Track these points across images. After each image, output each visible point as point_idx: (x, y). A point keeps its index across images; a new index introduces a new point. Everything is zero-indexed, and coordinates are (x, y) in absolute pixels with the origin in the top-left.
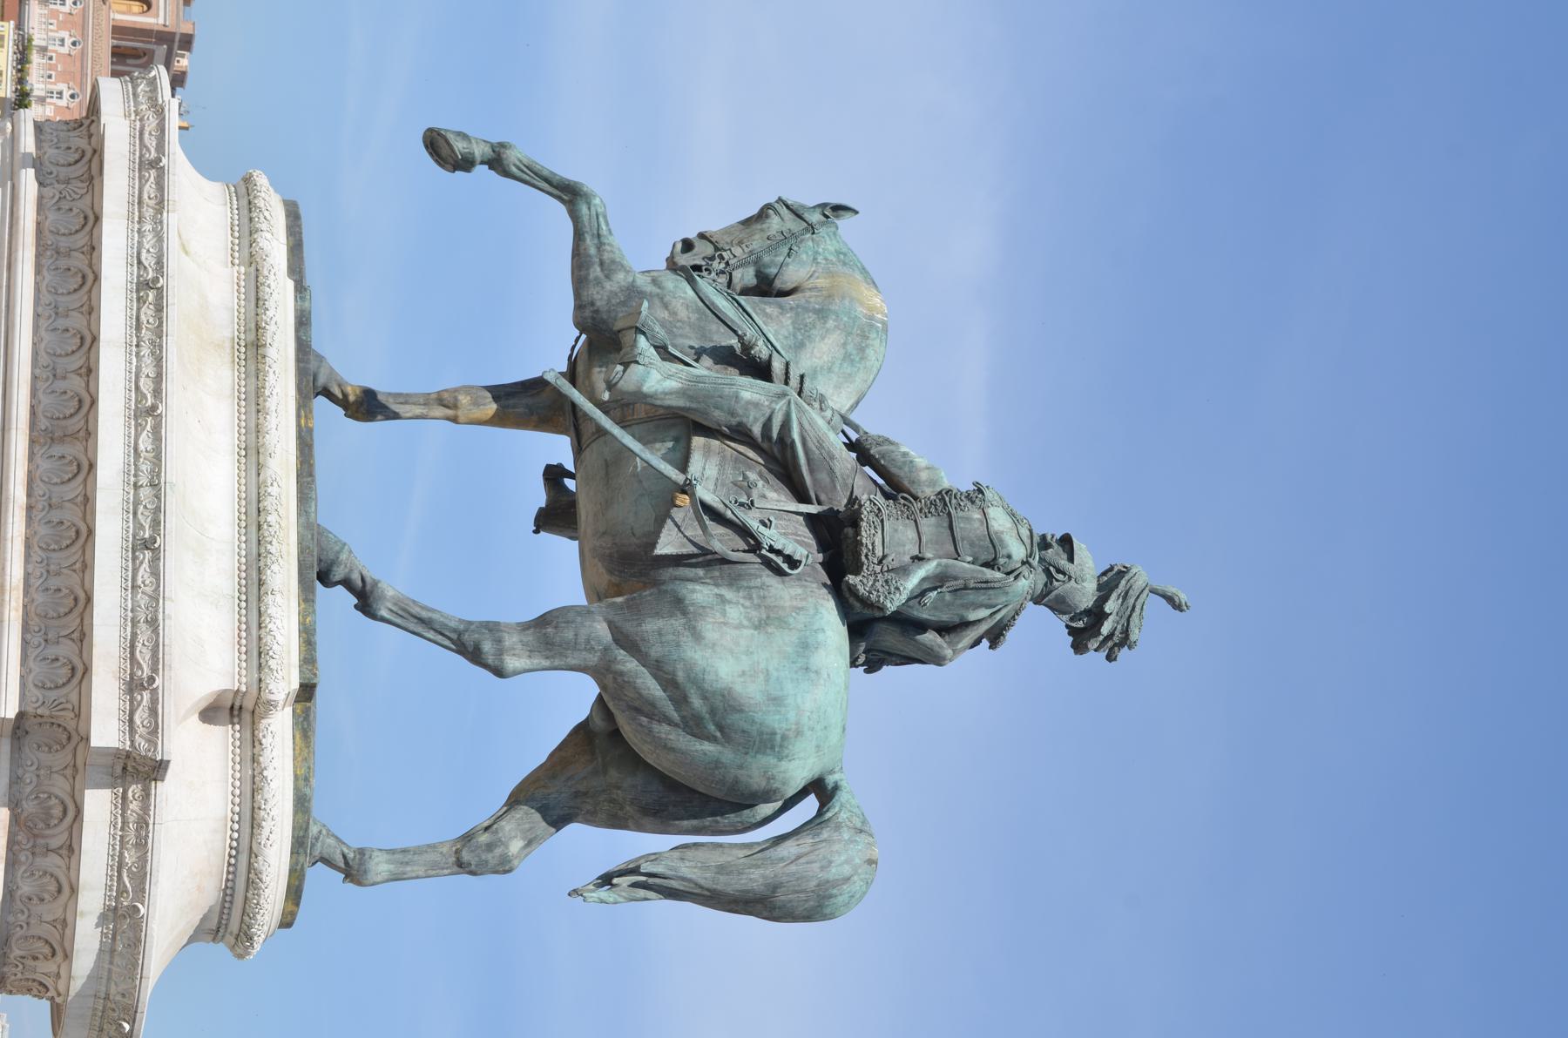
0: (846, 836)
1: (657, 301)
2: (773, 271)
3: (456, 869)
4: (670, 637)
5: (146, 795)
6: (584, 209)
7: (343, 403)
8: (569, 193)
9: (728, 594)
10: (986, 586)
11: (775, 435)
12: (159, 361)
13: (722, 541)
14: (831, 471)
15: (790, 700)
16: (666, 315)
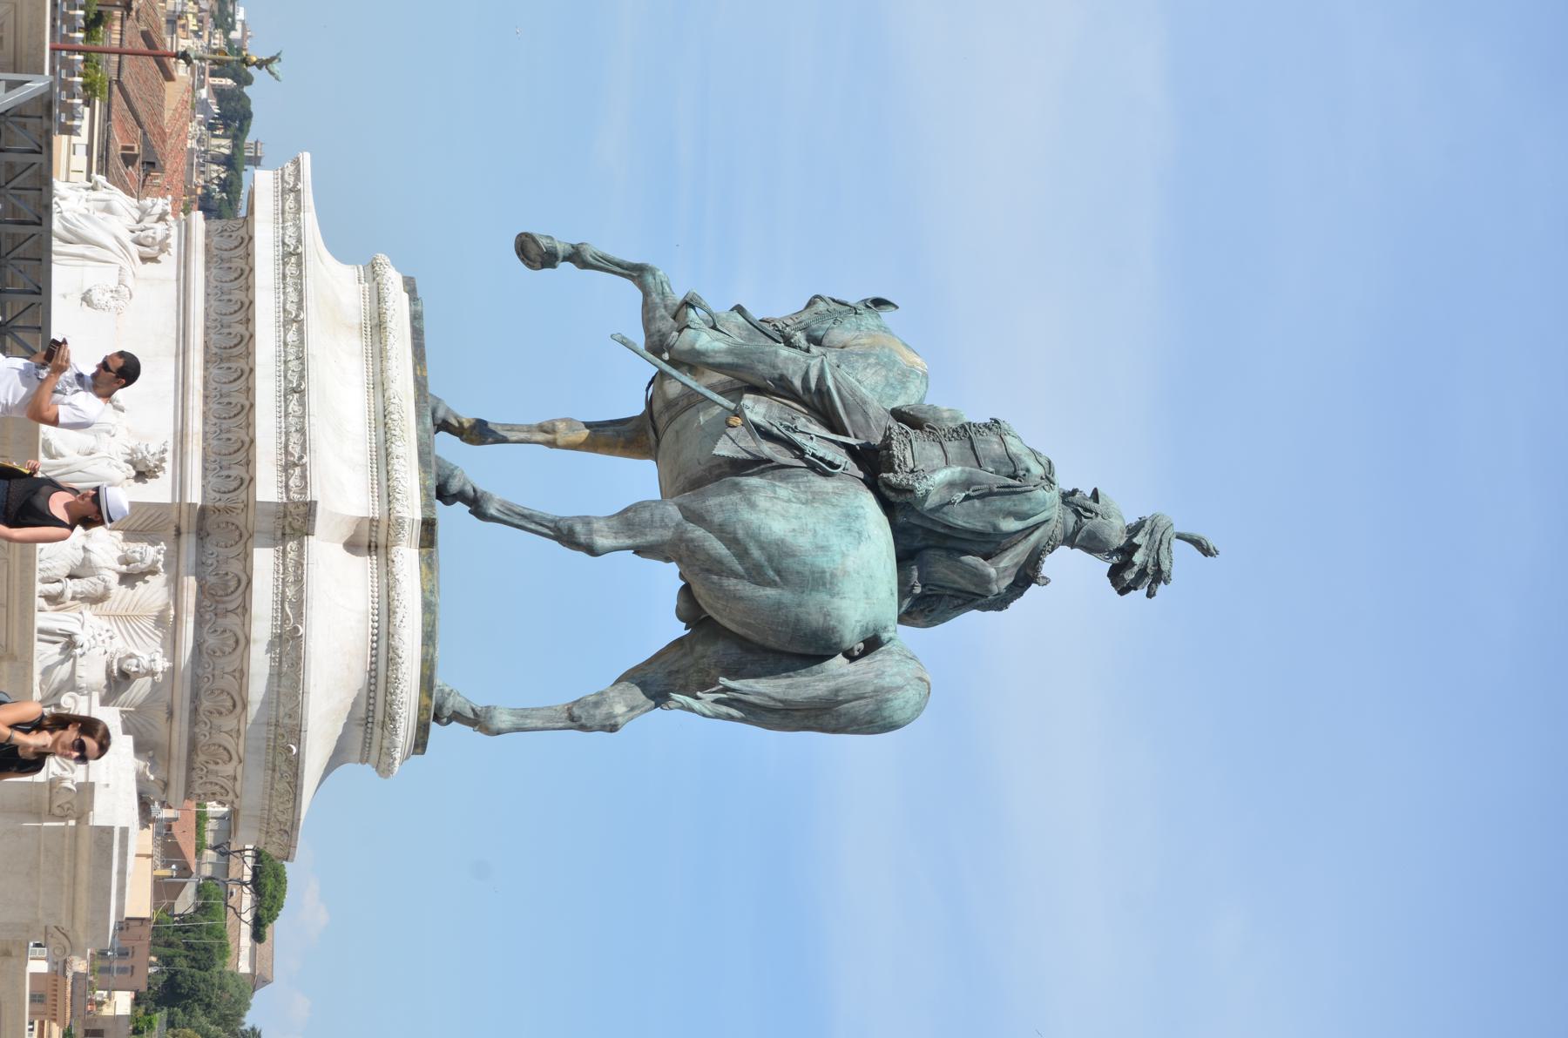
2: (821, 333)
3: (569, 723)
5: (301, 545)
6: (650, 279)
8: (636, 273)
11: (813, 385)
12: (300, 293)
14: (865, 413)
15: (836, 548)
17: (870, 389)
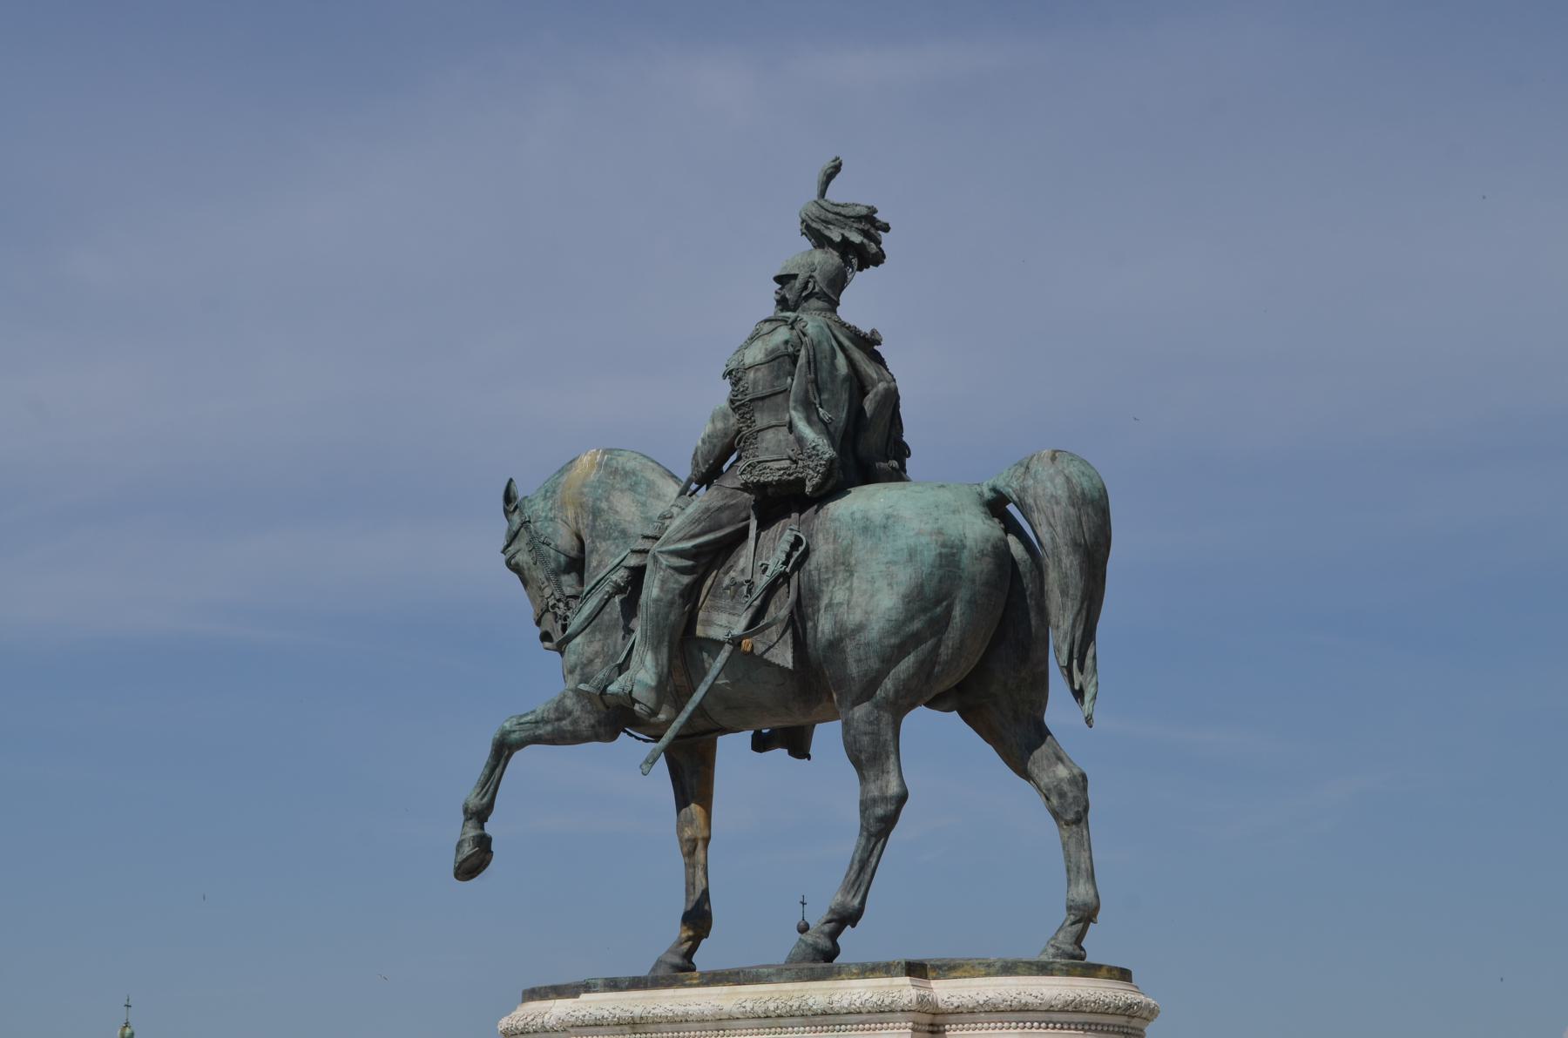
0: (1031, 482)
1: (587, 670)
2: (562, 558)
6: (515, 736)
7: (696, 941)
8: (503, 750)
9: (824, 601)
10: (813, 363)
11: (689, 563)
13: (780, 610)
15: (911, 542)
16: (598, 661)
17: (660, 509)
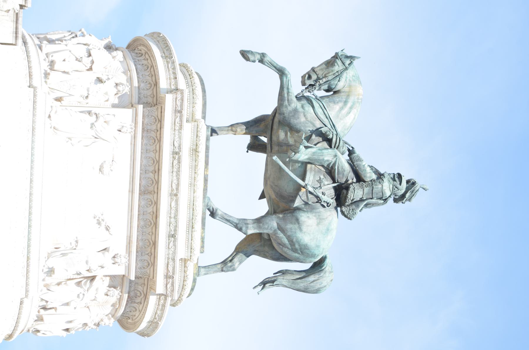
2: (333, 87)
4: (294, 230)
6: (285, 79)
8: (281, 72)
12: (178, 179)
